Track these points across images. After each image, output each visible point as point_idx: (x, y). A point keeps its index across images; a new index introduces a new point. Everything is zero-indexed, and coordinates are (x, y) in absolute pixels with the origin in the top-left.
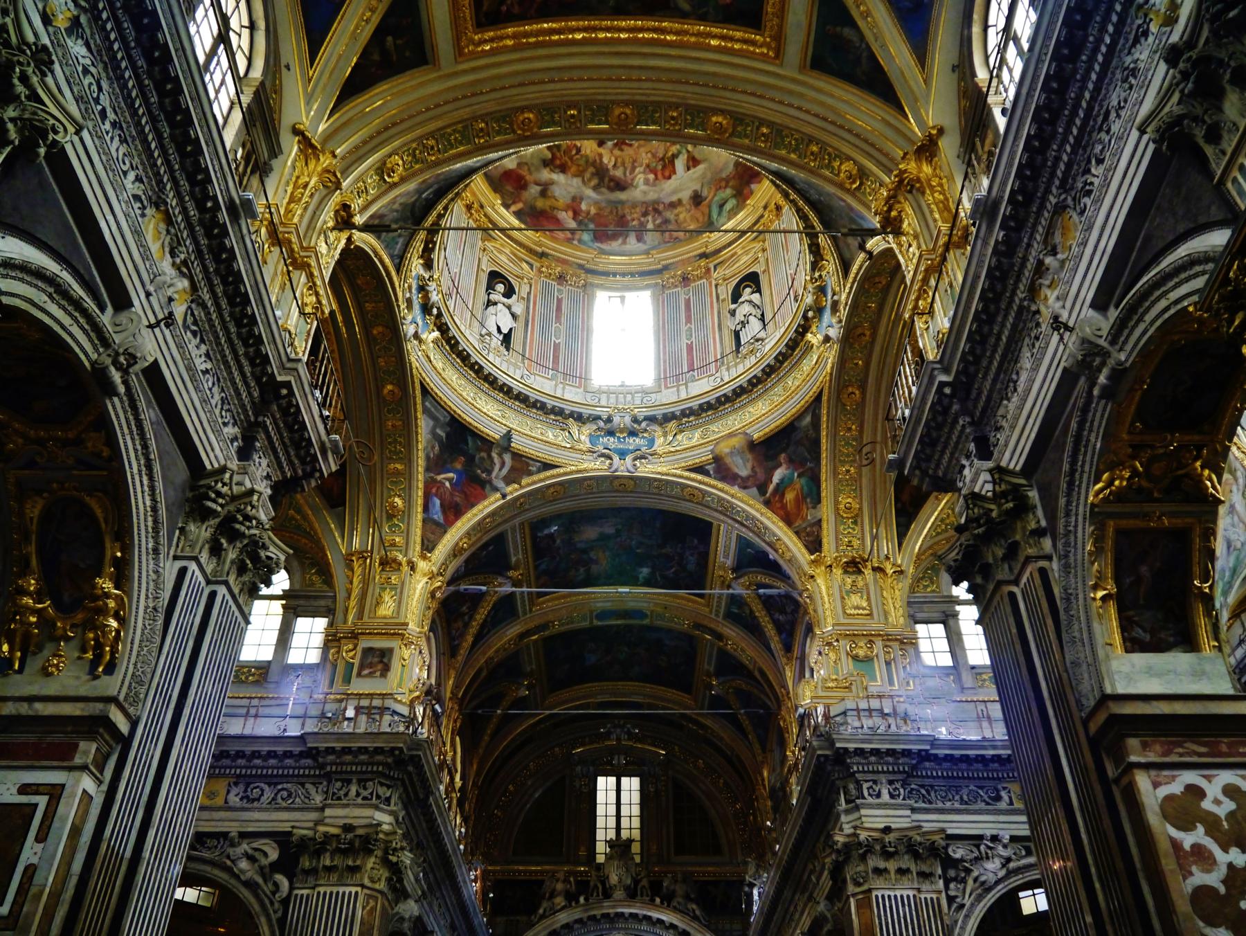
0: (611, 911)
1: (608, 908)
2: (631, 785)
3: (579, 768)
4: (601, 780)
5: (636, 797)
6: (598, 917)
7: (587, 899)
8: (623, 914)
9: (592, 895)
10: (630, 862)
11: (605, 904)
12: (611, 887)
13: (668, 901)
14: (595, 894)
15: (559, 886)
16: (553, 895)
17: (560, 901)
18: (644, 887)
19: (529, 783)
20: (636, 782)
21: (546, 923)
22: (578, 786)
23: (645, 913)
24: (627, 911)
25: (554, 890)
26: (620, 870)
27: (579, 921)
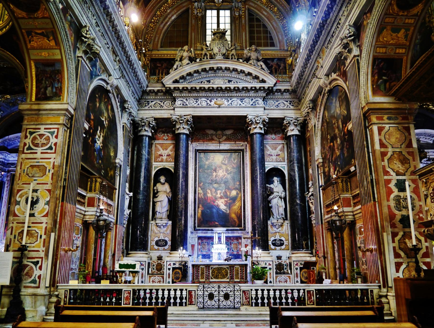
0: (215, 66)
1: (213, 64)
2: (225, 15)
3: (196, 4)
4: (209, 12)
5: (228, 20)
6: (208, 69)
7: (201, 60)
8: (221, 69)
9: (204, 58)
10: (225, 42)
11: (211, 62)
12: (214, 54)
13: (247, 60)
14: (205, 58)
15: (185, 54)
16: (181, 60)
17: (186, 61)
18: (233, 54)
19: (169, 11)
20: (228, 13)
21: (178, 71)
22: (196, 13)
23: (234, 67)
24: (223, 66)
25: (182, 56)
26: (219, 46)
27: (197, 72)
